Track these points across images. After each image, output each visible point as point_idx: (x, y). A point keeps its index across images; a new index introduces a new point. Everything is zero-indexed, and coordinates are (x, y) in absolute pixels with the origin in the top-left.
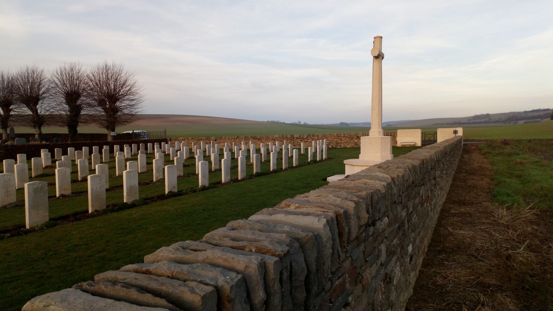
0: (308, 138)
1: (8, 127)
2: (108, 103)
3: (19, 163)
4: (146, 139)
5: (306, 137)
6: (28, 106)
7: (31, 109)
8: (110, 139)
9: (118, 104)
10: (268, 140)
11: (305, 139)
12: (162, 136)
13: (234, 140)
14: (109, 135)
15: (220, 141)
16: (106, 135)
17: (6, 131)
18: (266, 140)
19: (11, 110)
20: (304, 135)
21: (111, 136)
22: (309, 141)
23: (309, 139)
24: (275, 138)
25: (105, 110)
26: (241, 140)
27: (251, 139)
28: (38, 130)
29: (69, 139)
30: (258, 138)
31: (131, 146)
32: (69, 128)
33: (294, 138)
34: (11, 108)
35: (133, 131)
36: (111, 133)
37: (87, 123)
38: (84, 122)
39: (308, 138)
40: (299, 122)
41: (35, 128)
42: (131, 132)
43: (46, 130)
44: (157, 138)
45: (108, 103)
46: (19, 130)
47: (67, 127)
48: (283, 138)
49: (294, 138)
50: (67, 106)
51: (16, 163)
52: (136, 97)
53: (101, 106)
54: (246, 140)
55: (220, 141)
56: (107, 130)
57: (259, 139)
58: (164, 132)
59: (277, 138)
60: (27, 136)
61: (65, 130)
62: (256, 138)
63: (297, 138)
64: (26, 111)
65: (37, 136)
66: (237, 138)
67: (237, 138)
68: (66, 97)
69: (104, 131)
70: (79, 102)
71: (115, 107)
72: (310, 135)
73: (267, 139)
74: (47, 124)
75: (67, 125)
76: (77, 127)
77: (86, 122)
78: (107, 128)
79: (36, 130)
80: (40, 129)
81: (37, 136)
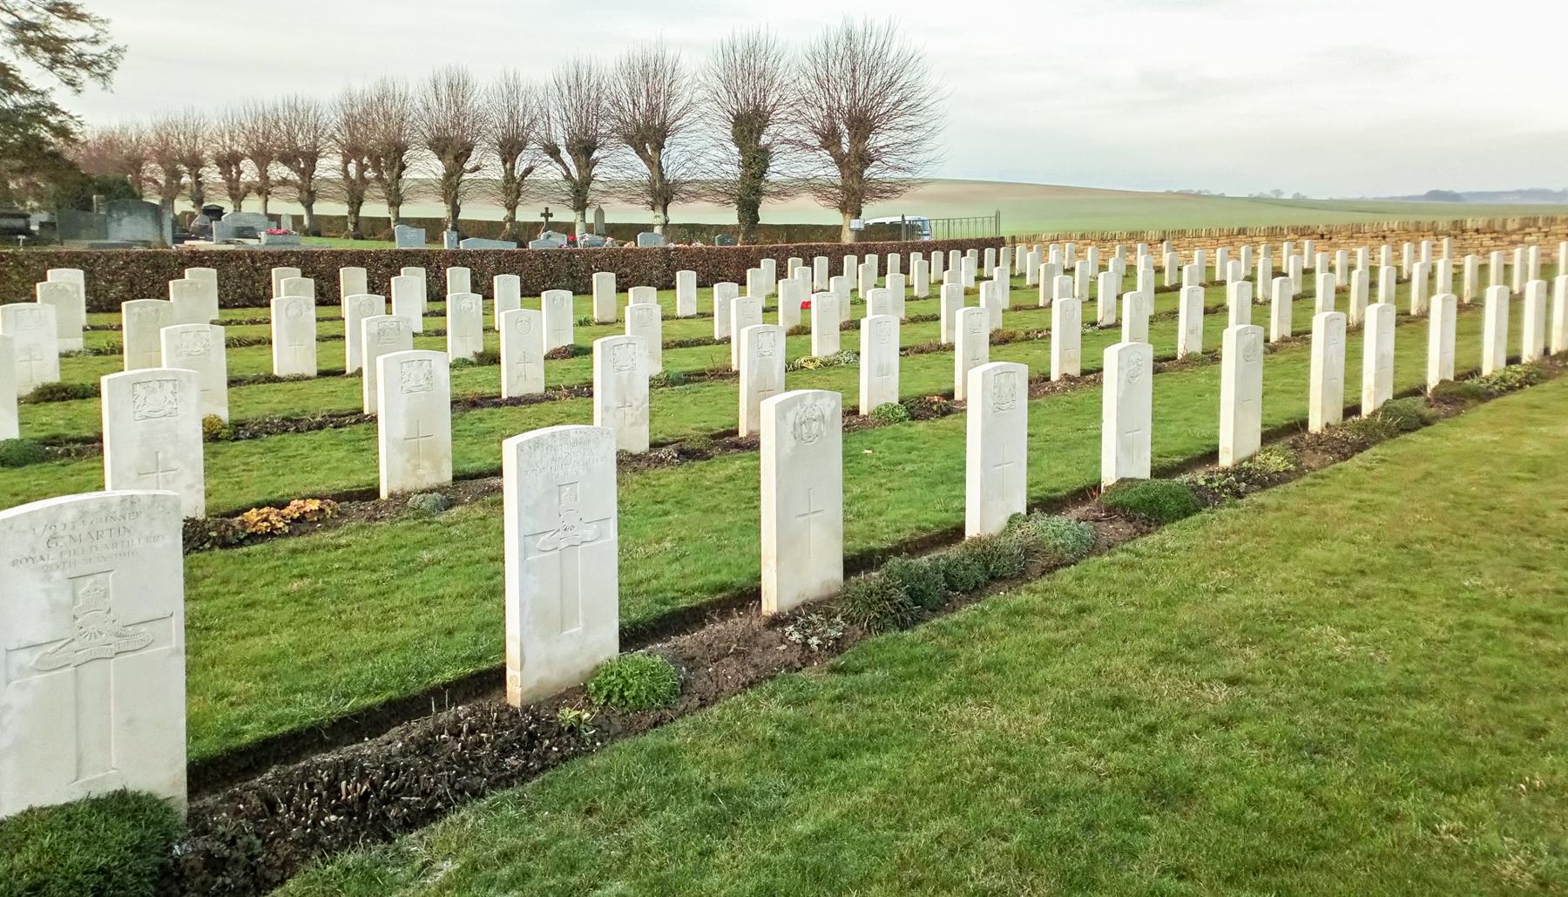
0: (1528, 230)
2: (845, 140)
4: (926, 239)
5: (1516, 226)
6: (641, 152)
7: (648, 161)
8: (847, 238)
9: (877, 141)
10: (1357, 238)
11: (1514, 232)
12: (987, 232)
13: (1228, 241)
14: (847, 229)
15: (1176, 242)
16: (839, 229)
17: (584, 215)
18: (1352, 237)
19: (595, 163)
20: (1509, 221)
21: (851, 230)
22: (1527, 239)
23: (1530, 234)
24: (1387, 233)
25: (840, 161)
26: (1255, 239)
27: (1292, 236)
28: (662, 214)
30: (1319, 231)
31: (927, 257)
32: (741, 210)
33: (1464, 231)
34: (596, 154)
35: (903, 216)
36: (853, 221)
37: (785, 194)
38: (777, 194)
39: (1528, 230)
40: (1277, 192)
41: (653, 209)
42: (899, 219)
43: (680, 213)
44: (980, 237)
45: (845, 140)
46: (619, 213)
47: (736, 206)
48: (1418, 230)
49: (1464, 231)
50: (736, 150)
51: (742, 293)
52: (922, 120)
53: (826, 149)
54: (1273, 238)
55: (1176, 242)
57: (1322, 236)
58: (994, 219)
59: (1393, 231)
60: (631, 231)
61: (729, 216)
62: (1313, 233)
63: (1477, 231)
65: (657, 230)
66: (1239, 233)
67: (1239, 233)
69: (830, 216)
71: (865, 150)
72: (1536, 220)
73: (1355, 235)
76: (758, 207)
77: (783, 192)
78: (843, 208)
79: (657, 214)
80: (665, 212)
81: (657, 230)
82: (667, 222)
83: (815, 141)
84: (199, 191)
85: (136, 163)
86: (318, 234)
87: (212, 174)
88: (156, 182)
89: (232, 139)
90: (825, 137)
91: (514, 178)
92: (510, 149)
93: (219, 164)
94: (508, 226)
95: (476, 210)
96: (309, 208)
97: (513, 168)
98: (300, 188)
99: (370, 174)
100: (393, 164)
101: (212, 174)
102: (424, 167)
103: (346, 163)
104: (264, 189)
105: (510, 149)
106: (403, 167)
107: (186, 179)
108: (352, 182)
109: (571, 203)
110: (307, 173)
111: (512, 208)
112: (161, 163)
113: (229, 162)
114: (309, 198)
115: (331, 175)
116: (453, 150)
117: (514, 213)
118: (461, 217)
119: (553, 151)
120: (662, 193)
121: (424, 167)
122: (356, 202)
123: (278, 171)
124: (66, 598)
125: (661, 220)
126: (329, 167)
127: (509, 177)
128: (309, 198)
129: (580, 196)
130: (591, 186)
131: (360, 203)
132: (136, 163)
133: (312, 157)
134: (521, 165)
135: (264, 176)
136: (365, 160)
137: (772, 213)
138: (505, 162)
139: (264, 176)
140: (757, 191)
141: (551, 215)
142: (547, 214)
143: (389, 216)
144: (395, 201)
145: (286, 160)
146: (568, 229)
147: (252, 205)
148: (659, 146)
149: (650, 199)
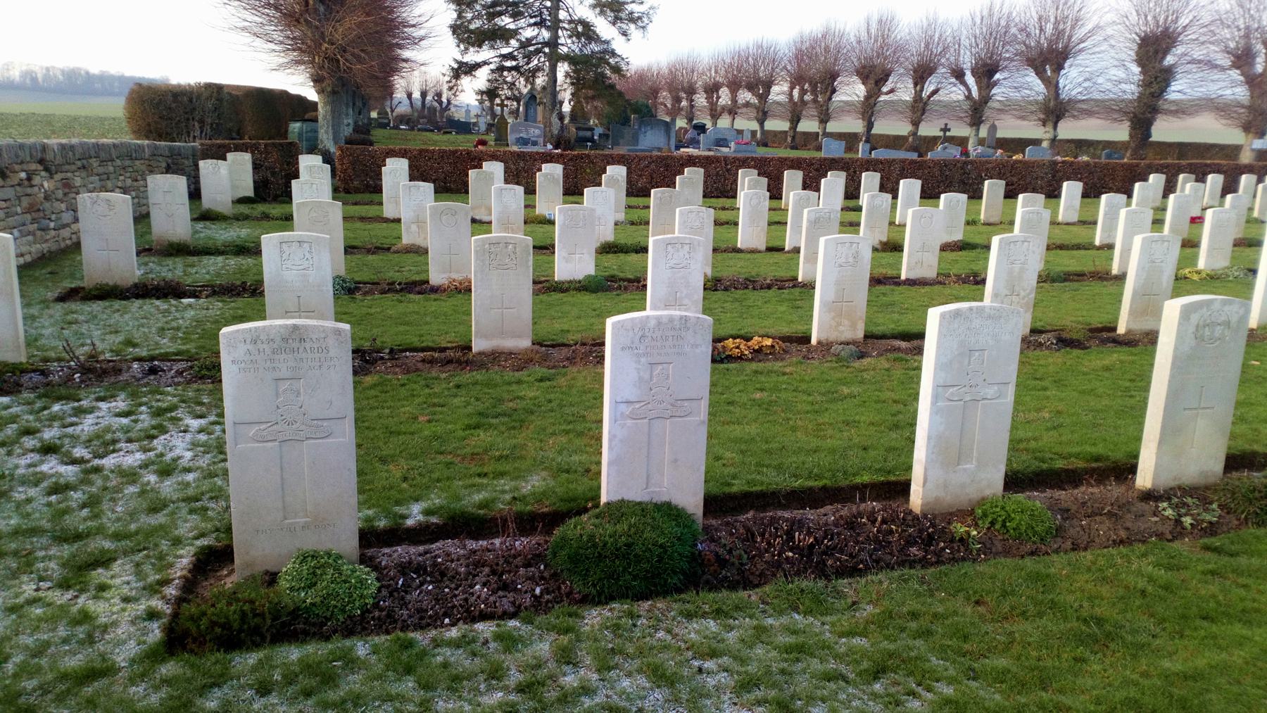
1: (982, 121)
3: (1137, 205)
6: (1040, 73)
8: (1246, 158)
16: (1235, 150)
17: (978, 130)
19: (995, 84)
21: (1253, 150)
29: (1128, 155)
32: (1133, 128)
34: (997, 76)
37: (1184, 113)
43: (1069, 130)
46: (1010, 128)
47: (1129, 123)
50: (1136, 69)
51: (1129, 204)
53: (1238, 68)
56: (1243, 134)
60: (1020, 144)
61: (1120, 133)
64: (1033, 86)
65: (1045, 144)
68: (1140, 46)
70: (1169, 60)
74: (1074, 117)
75: (1131, 120)
77: (1182, 110)
78: (1247, 128)
79: (1047, 129)
80: (1055, 128)
81: (1045, 144)
82: (1055, 137)
83: (1225, 61)
84: (692, 112)
85: (655, 92)
86: (766, 145)
87: (701, 100)
88: (666, 106)
89: (716, 72)
90: (1238, 57)
91: (921, 98)
92: (922, 73)
93: (706, 92)
94: (911, 139)
95: (885, 126)
96: (762, 124)
97: (922, 90)
98: (757, 108)
99: (808, 97)
100: (826, 88)
101: (701, 100)
102: (852, 90)
103: (792, 88)
104: (733, 111)
105: (922, 73)
106: (834, 91)
107: (684, 103)
108: (795, 104)
109: (968, 120)
110: (763, 97)
111: (916, 124)
112: (670, 92)
113: (712, 90)
114: (762, 116)
115: (783, 98)
116: (875, 76)
117: (917, 129)
118: (874, 131)
119: (959, 75)
120: (1055, 110)
121: (852, 90)
122: (795, 120)
123: (745, 96)
124: (647, 376)
125: (1050, 136)
126: (779, 92)
127: (918, 98)
128: (762, 116)
129: (977, 112)
130: (989, 104)
131: (798, 121)
132: (655, 92)
133: (768, 85)
134: (929, 88)
135: (734, 100)
136: (806, 86)
137: (1164, 131)
138: (916, 84)
139: (734, 100)
140: (1154, 109)
141: (949, 130)
142: (945, 129)
143: (818, 130)
144: (824, 119)
145: (751, 87)
146: (962, 142)
147: (724, 122)
148: (1059, 67)
149: (1042, 116)
